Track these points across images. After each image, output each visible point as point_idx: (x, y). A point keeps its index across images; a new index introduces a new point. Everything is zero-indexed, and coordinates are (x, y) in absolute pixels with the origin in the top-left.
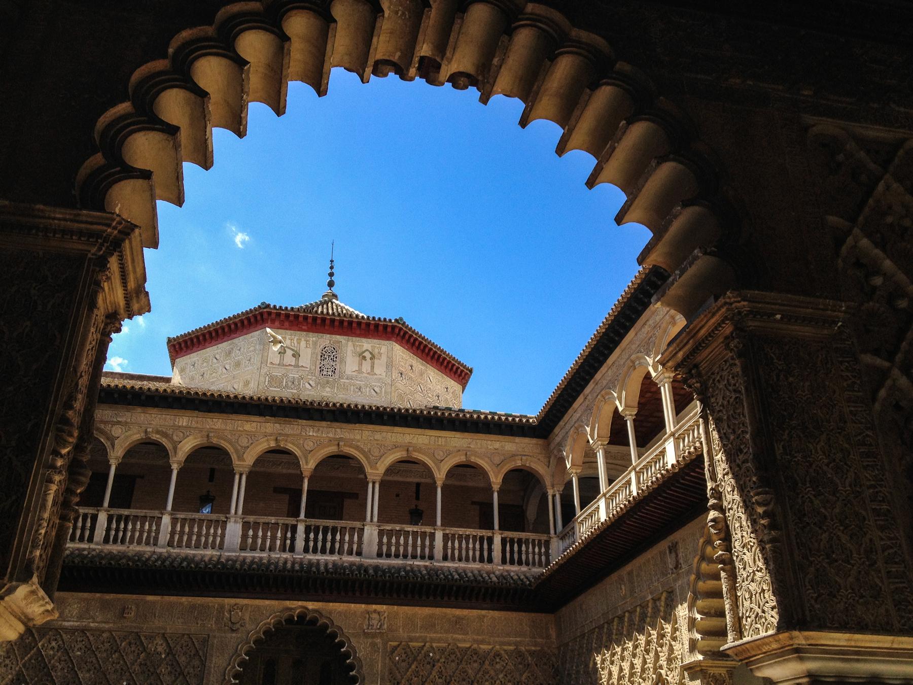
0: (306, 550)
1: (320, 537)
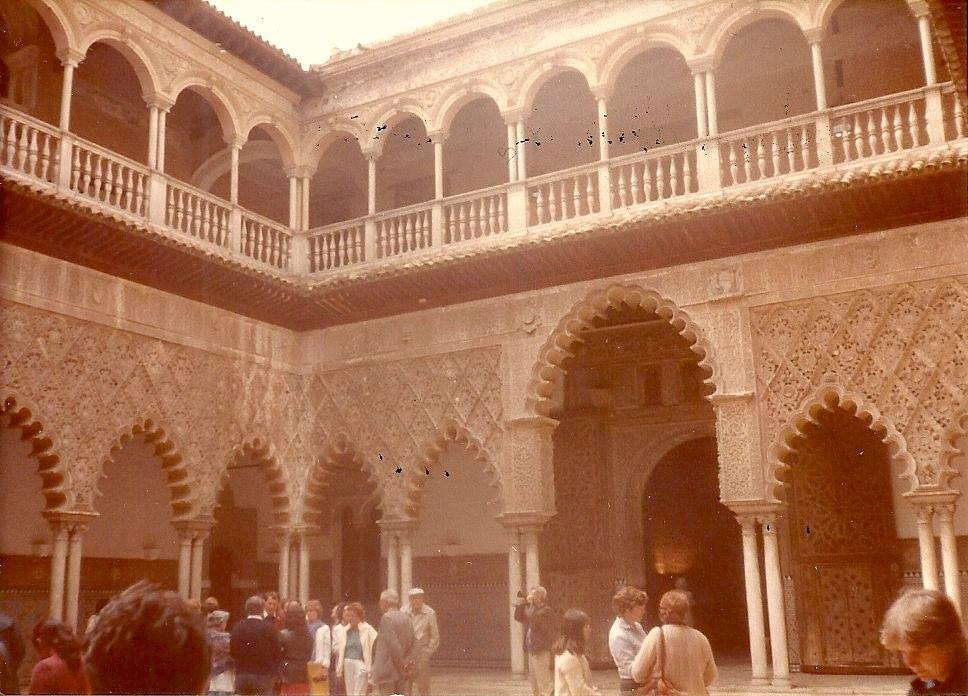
0: (616, 204)
1: (633, 179)
